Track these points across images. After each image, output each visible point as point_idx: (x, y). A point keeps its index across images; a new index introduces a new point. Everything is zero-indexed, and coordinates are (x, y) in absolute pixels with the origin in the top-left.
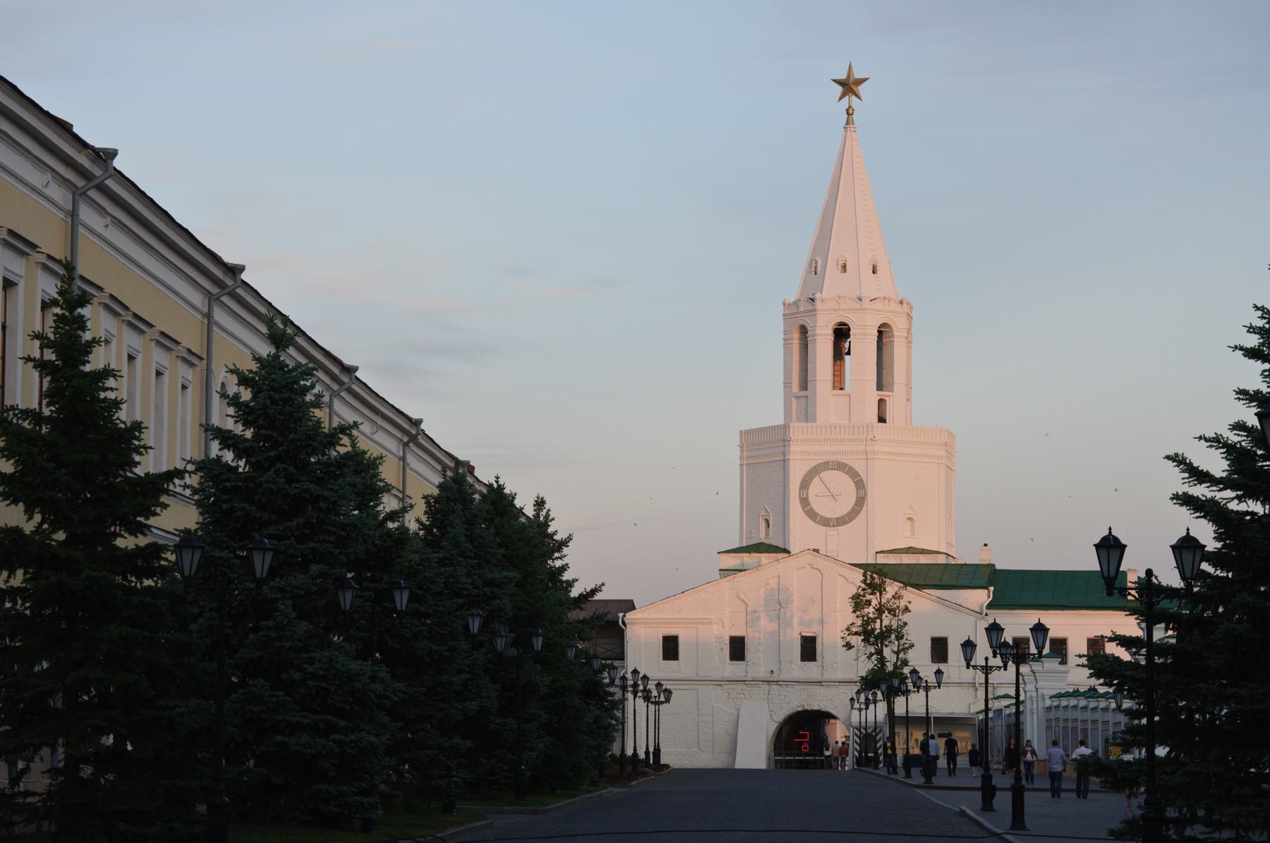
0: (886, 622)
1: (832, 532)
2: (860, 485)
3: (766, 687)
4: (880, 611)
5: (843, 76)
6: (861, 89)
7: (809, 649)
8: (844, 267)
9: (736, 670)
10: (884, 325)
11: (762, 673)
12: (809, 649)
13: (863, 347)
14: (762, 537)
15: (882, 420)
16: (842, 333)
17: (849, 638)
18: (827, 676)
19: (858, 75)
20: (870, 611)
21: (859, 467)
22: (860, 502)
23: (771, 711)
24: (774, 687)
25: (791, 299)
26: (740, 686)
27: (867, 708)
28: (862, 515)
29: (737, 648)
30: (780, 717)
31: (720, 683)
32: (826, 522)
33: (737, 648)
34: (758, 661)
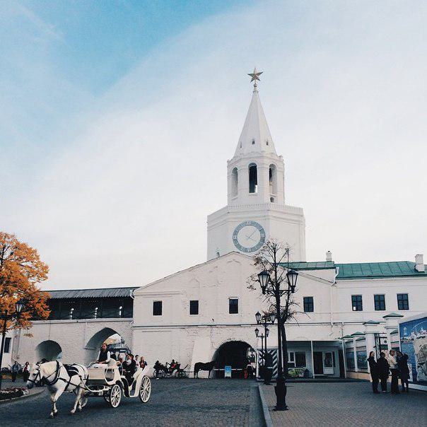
2: (262, 231)
3: (209, 328)
6: (260, 77)
7: (234, 307)
8: (253, 143)
9: (194, 319)
10: (272, 165)
12: (234, 307)
13: (263, 175)
15: (272, 200)
16: (253, 171)
18: (244, 322)
26: (195, 328)
29: (194, 308)
30: (217, 346)
31: (183, 327)
33: (194, 308)
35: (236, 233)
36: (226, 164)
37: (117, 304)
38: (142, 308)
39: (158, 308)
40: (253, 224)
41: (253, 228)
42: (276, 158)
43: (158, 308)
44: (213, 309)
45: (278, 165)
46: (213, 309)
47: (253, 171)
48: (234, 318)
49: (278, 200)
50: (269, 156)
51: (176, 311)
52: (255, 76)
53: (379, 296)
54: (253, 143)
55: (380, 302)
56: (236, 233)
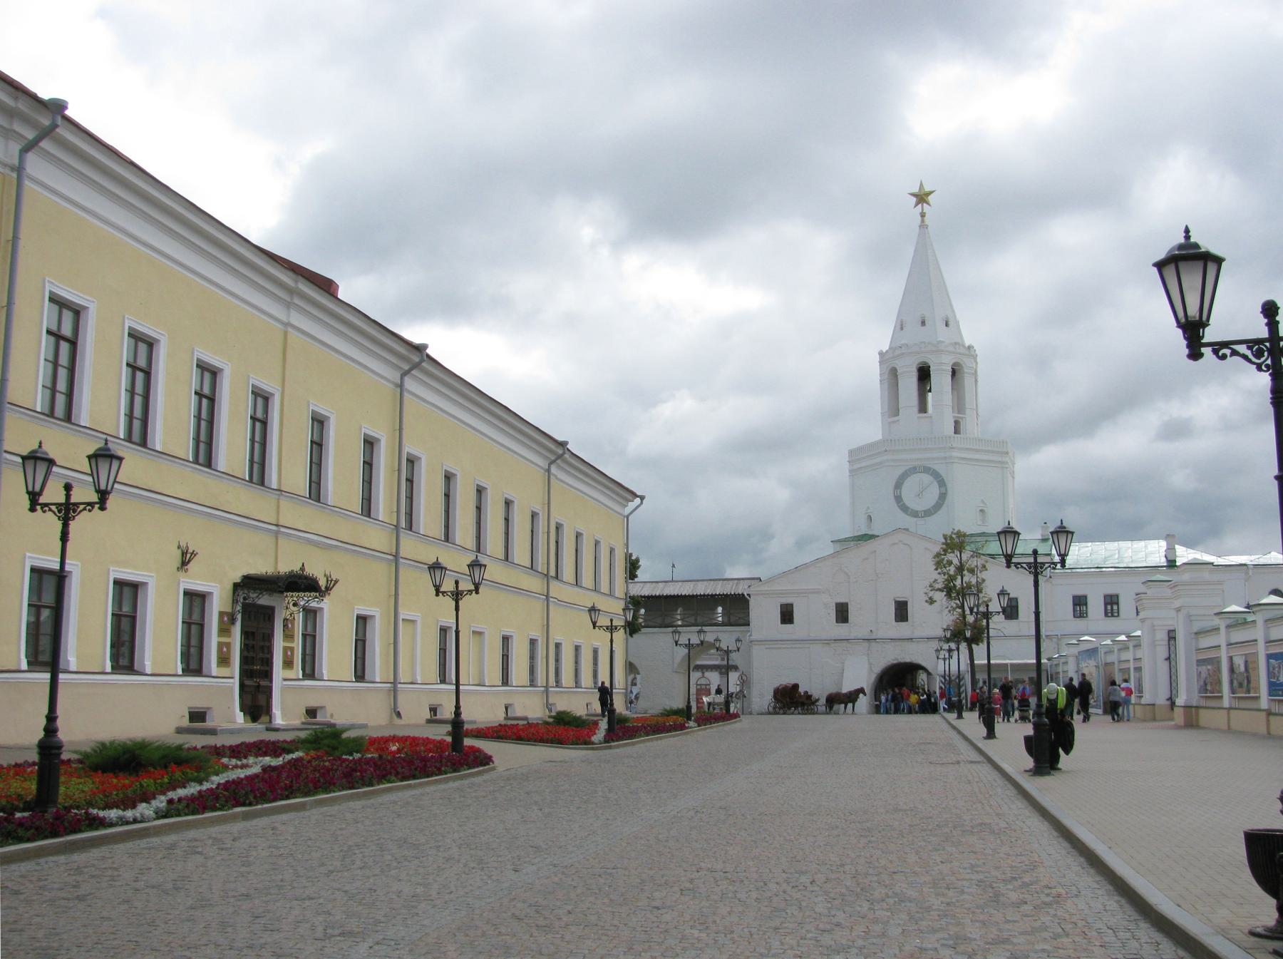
0: (966, 579)
1: (920, 521)
2: (942, 483)
3: (866, 644)
4: (960, 569)
5: (916, 190)
6: (930, 198)
7: (902, 611)
8: (923, 323)
9: (841, 630)
10: (955, 364)
11: (864, 633)
12: (902, 611)
13: (940, 380)
14: (864, 531)
15: (957, 431)
16: (924, 374)
17: (931, 594)
18: (918, 633)
19: (927, 189)
20: (952, 570)
21: (941, 469)
22: (943, 496)
23: (870, 664)
24: (873, 644)
25: (885, 348)
26: (844, 644)
27: (950, 657)
28: (944, 508)
29: (842, 613)
30: (879, 667)
31: (827, 642)
32: (915, 514)
33: (842, 613)
34: (860, 623)
35: (898, 485)
36: (877, 358)
37: (736, 607)
38: (763, 614)
39: (787, 615)
40: (927, 470)
41: (927, 478)
42: (962, 350)
43: (787, 615)
44: (872, 615)
45: (967, 363)
46: (872, 615)
47: (924, 374)
48: (903, 629)
49: (969, 425)
50: (951, 349)
51: (815, 617)
52: (922, 198)
53: (1111, 596)
54: (923, 323)
55: (1111, 603)
56: (898, 485)
